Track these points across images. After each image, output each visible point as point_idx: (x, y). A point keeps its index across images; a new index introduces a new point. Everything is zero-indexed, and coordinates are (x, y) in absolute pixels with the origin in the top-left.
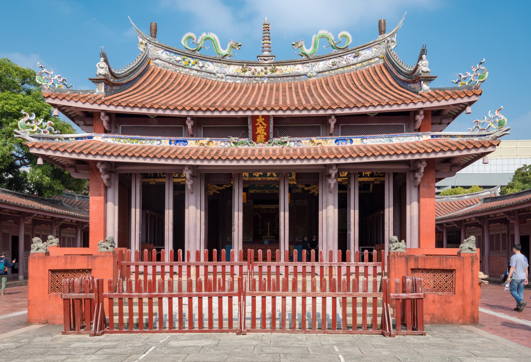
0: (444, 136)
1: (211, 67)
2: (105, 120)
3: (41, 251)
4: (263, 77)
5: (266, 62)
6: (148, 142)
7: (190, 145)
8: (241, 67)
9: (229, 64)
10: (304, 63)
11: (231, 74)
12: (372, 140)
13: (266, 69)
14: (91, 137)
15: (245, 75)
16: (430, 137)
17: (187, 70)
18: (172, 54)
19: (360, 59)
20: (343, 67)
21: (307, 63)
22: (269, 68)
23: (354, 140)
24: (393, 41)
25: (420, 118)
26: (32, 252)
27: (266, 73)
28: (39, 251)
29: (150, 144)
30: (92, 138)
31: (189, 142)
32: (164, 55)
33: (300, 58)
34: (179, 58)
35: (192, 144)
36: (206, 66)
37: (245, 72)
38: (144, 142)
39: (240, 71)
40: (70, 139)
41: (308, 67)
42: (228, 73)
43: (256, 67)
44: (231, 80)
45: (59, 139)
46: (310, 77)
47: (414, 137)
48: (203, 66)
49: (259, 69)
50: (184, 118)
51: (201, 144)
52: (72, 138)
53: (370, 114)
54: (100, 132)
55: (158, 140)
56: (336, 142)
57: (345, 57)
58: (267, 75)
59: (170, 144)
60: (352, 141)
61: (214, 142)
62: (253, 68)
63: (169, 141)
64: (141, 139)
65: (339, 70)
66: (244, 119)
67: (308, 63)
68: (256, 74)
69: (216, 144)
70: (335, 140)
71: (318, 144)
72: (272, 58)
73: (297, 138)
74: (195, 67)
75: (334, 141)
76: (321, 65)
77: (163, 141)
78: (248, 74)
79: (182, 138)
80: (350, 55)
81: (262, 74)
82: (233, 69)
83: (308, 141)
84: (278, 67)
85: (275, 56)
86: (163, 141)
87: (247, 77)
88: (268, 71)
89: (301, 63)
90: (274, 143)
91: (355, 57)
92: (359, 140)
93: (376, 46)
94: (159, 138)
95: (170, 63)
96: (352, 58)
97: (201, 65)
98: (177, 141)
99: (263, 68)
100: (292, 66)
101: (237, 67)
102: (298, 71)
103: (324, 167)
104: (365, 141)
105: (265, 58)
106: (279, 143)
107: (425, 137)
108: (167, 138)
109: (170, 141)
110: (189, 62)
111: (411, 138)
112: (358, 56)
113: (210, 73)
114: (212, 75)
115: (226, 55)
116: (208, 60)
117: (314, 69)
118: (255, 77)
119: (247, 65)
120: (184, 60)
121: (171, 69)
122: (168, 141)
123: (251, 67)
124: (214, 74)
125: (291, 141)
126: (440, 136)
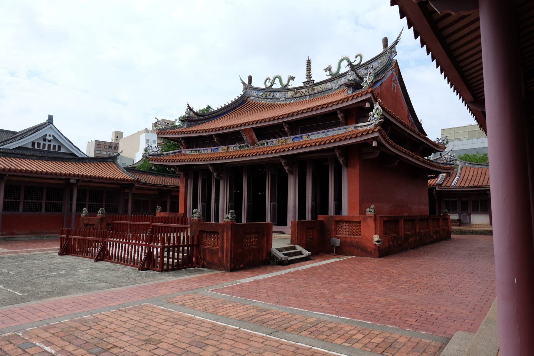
0: (358, 126)
1: (278, 95)
2: (182, 142)
3: (84, 215)
4: (306, 96)
5: (308, 85)
9: (287, 91)
11: (289, 97)
12: (315, 135)
13: (308, 89)
15: (297, 96)
16: (353, 129)
17: (266, 99)
22: (310, 88)
23: (303, 137)
24: (394, 51)
25: (340, 116)
26: (82, 215)
27: (308, 93)
29: (203, 153)
32: (254, 93)
33: (330, 77)
34: (261, 93)
35: (221, 150)
36: (275, 95)
37: (296, 94)
39: (293, 94)
40: (169, 154)
41: (334, 83)
42: (287, 97)
43: (302, 90)
44: (288, 101)
45: (163, 155)
46: (336, 89)
47: (343, 130)
48: (273, 96)
49: (304, 90)
50: (211, 136)
52: (170, 153)
53: (317, 116)
54: (184, 149)
58: (309, 94)
61: (230, 148)
62: (301, 90)
66: (238, 132)
67: (334, 80)
68: (303, 94)
70: (292, 139)
72: (311, 82)
74: (270, 97)
77: (208, 150)
78: (298, 95)
80: (362, 69)
82: (290, 94)
83: (277, 141)
84: (315, 87)
86: (208, 150)
87: (297, 97)
88: (310, 91)
90: (259, 146)
91: (365, 69)
93: (380, 58)
94: (207, 148)
95: (257, 97)
96: (363, 70)
97: (272, 95)
98: (215, 149)
99: (306, 90)
100: (324, 84)
101: (292, 92)
102: (327, 87)
104: (311, 137)
105: (307, 83)
106: (261, 144)
107: (350, 128)
108: (210, 148)
110: (267, 94)
111: (341, 130)
112: (367, 68)
113: (278, 99)
114: (278, 100)
115: (286, 86)
117: (338, 83)
118: (302, 96)
120: (264, 93)
121: (257, 101)
122: (210, 150)
123: (299, 90)
124: (279, 99)
125: (267, 143)
126: (361, 126)
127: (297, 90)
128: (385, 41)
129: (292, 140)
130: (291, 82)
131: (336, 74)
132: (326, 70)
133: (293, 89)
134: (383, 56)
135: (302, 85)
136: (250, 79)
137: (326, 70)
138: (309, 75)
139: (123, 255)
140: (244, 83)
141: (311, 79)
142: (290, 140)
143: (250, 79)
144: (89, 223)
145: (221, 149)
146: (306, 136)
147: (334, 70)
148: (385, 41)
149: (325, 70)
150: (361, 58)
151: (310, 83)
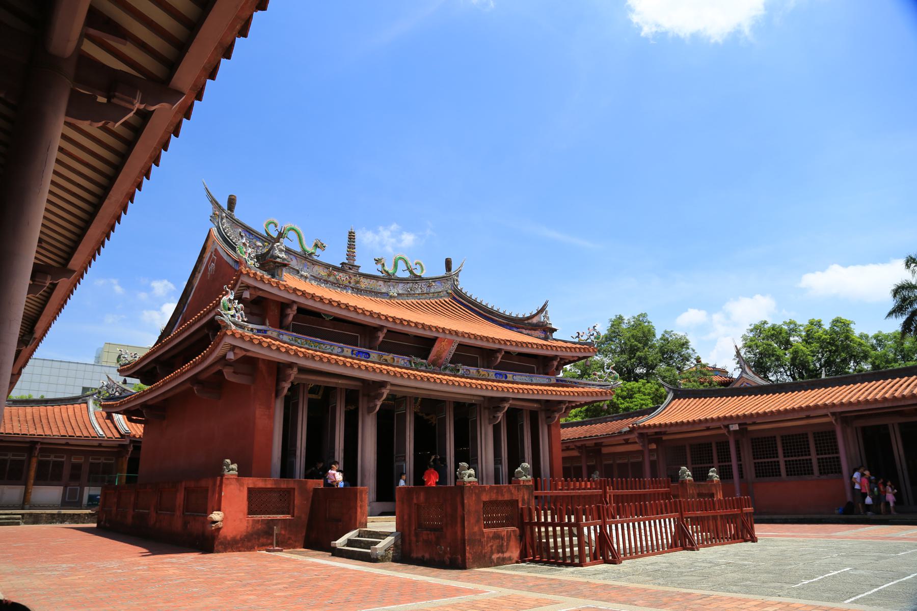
2: (292, 313)
6: (328, 347)
7: (372, 359)
8: (326, 270)
10: (385, 282)
12: (519, 377)
13: (350, 277)
14: (265, 331)
16: (555, 382)
18: (251, 237)
19: (432, 290)
20: (419, 294)
21: (388, 282)
22: (353, 278)
23: (508, 375)
28: (470, 478)
30: (266, 333)
31: (372, 355)
33: (380, 274)
38: (324, 347)
51: (384, 359)
55: (339, 347)
56: (495, 375)
57: (420, 284)
59: (352, 354)
60: (506, 377)
63: (351, 350)
64: (321, 344)
65: (415, 295)
69: (398, 362)
71: (483, 375)
73: (466, 367)
75: (494, 374)
76: (400, 289)
78: (331, 279)
79: (365, 349)
81: (346, 283)
85: (359, 267)
89: (383, 281)
92: (511, 375)
93: (443, 281)
94: (342, 344)
98: (359, 352)
100: (374, 280)
101: (321, 268)
103: (482, 399)
105: (351, 267)
108: (349, 346)
109: (352, 351)
116: (292, 253)
119: (333, 270)
122: (350, 351)
127: (333, 270)
128: (448, 263)
129: (494, 375)
130: (318, 252)
131: (394, 274)
132: (378, 261)
133: (327, 266)
134: (447, 280)
135: (340, 266)
136: (232, 202)
137: (378, 261)
138: (351, 255)
139: (660, 541)
140: (214, 202)
141: (356, 263)
142: (492, 375)
143: (232, 202)
144: (500, 498)
145: (376, 356)
146: (511, 375)
147: (389, 268)
148: (448, 263)
149: (375, 260)
150: (422, 270)
151: (348, 267)
